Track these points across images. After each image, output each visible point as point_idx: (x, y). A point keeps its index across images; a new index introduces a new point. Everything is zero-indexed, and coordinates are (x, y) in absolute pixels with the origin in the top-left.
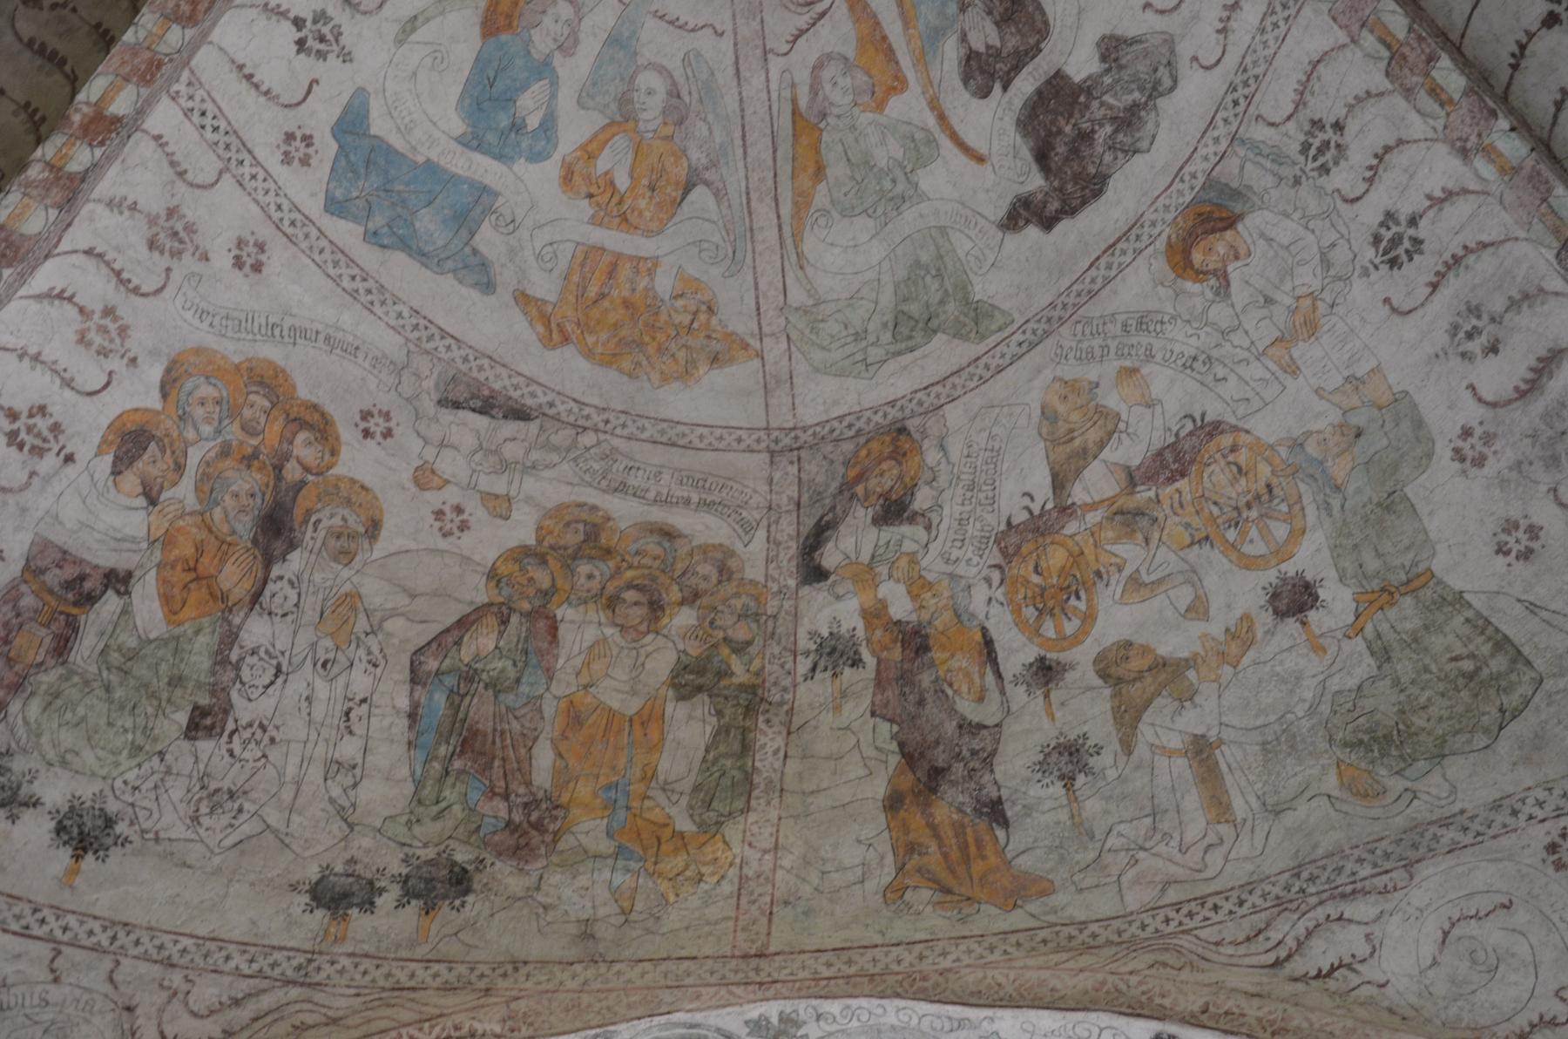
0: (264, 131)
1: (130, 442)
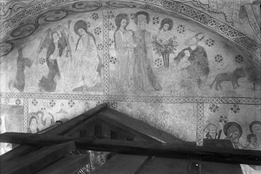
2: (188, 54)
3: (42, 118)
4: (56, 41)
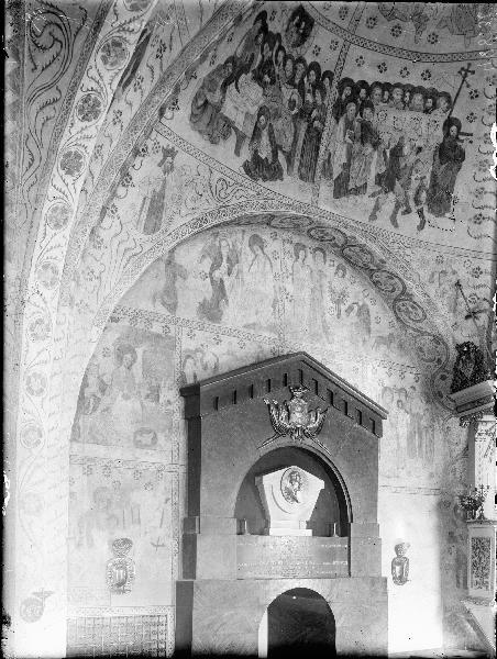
2: (356, 308)
3: (202, 359)
4: (225, 252)
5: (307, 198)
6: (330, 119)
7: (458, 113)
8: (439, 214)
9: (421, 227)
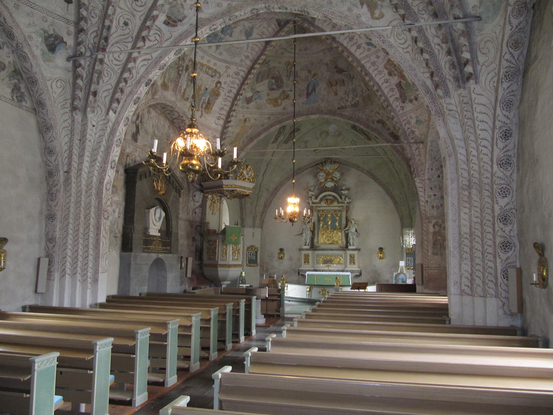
0: (367, 53)
1: (390, 74)
5: (173, 99)
6: (184, 71)
7: (222, 80)
8: (207, 113)
9: (201, 117)
